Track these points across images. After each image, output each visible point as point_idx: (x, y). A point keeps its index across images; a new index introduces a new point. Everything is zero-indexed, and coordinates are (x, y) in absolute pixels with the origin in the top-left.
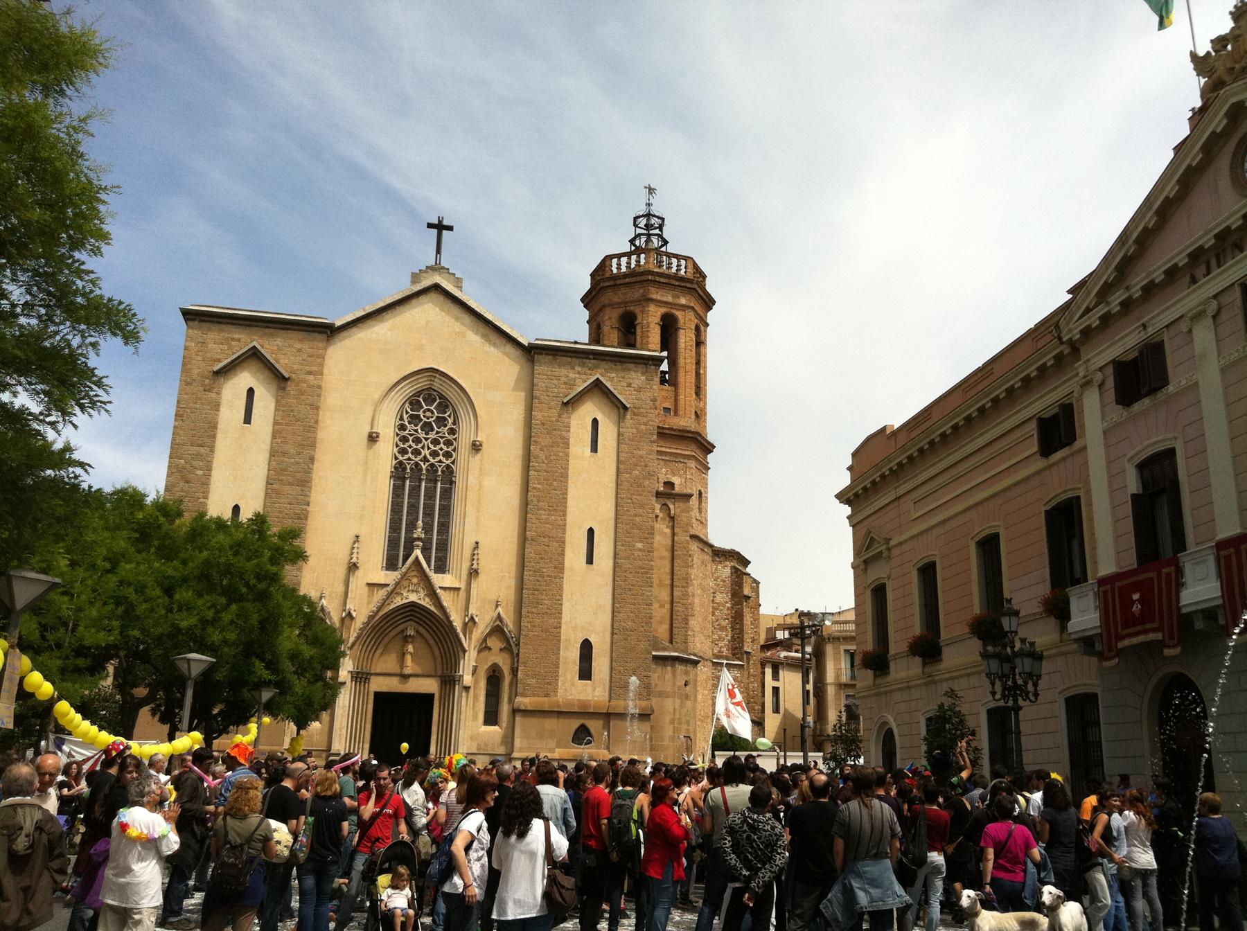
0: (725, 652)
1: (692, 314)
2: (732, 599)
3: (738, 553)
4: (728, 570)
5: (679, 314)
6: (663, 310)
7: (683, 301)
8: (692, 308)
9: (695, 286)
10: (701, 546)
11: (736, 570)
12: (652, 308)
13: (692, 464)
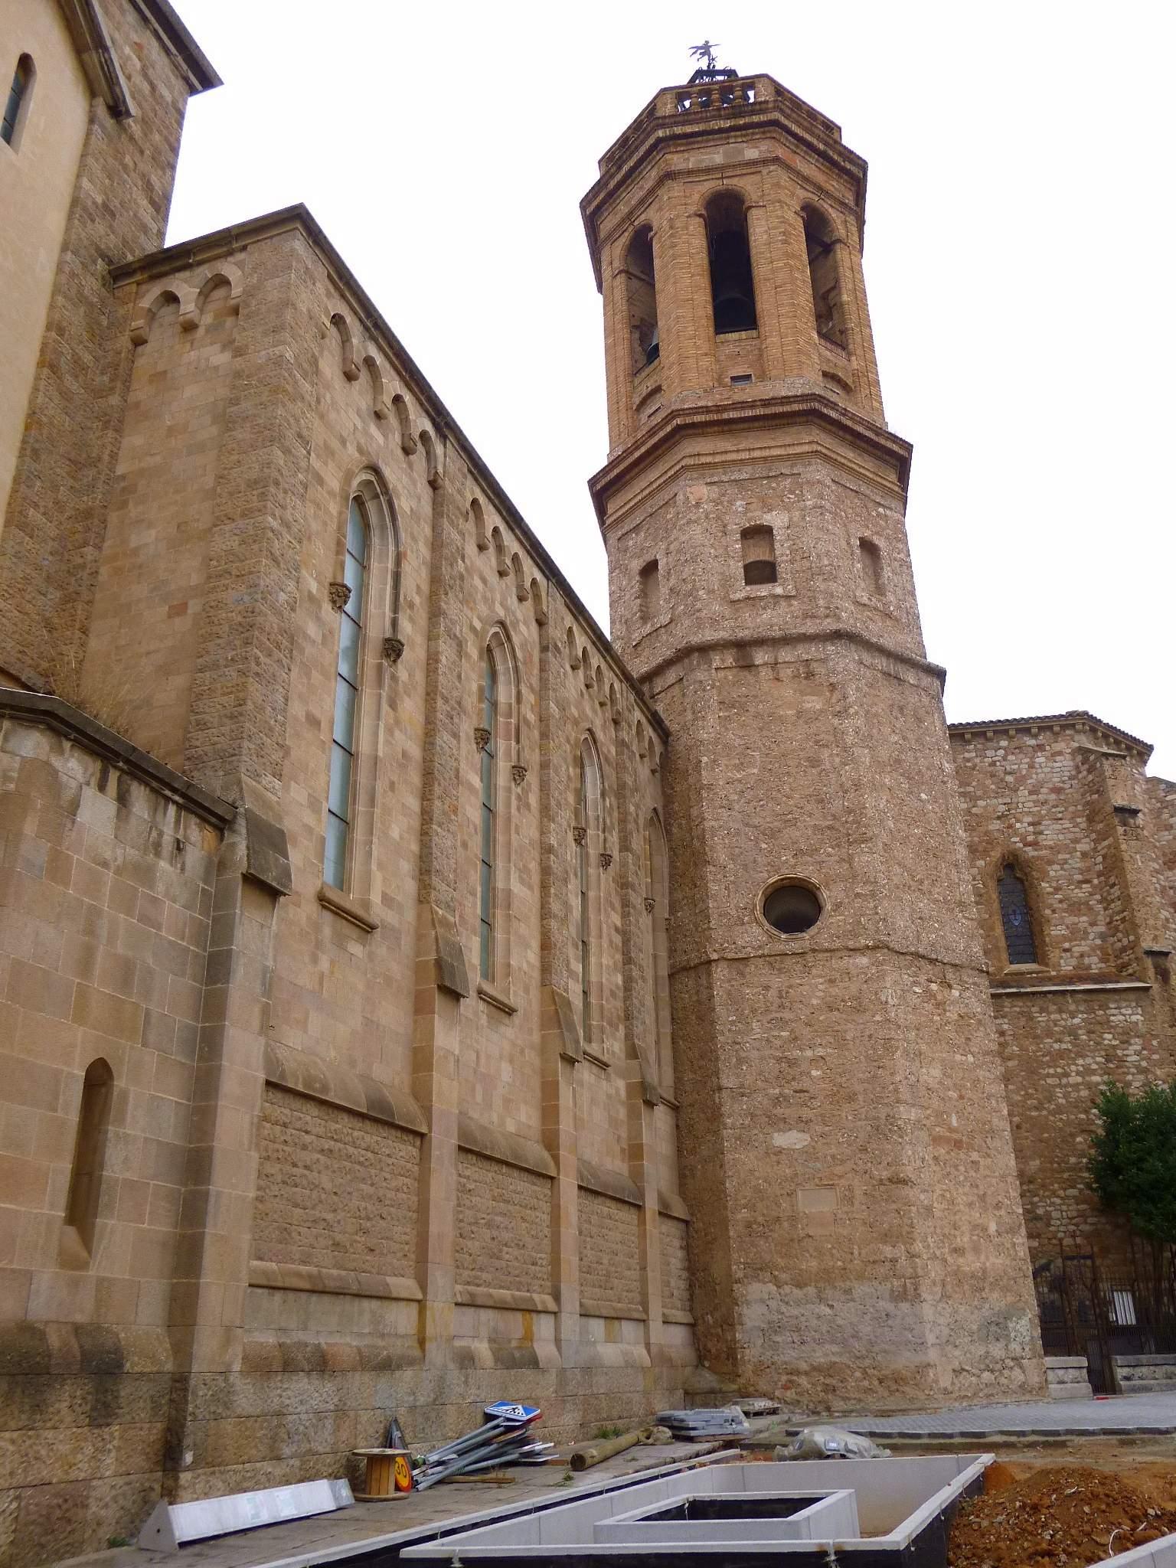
0: (1095, 965)
1: (783, 176)
2: (1089, 830)
3: (1085, 716)
4: (1065, 763)
5: (747, 185)
6: (709, 186)
7: (752, 153)
8: (776, 160)
9: (776, 115)
10: (881, 662)
11: (1083, 751)
12: (674, 190)
13: (819, 472)
